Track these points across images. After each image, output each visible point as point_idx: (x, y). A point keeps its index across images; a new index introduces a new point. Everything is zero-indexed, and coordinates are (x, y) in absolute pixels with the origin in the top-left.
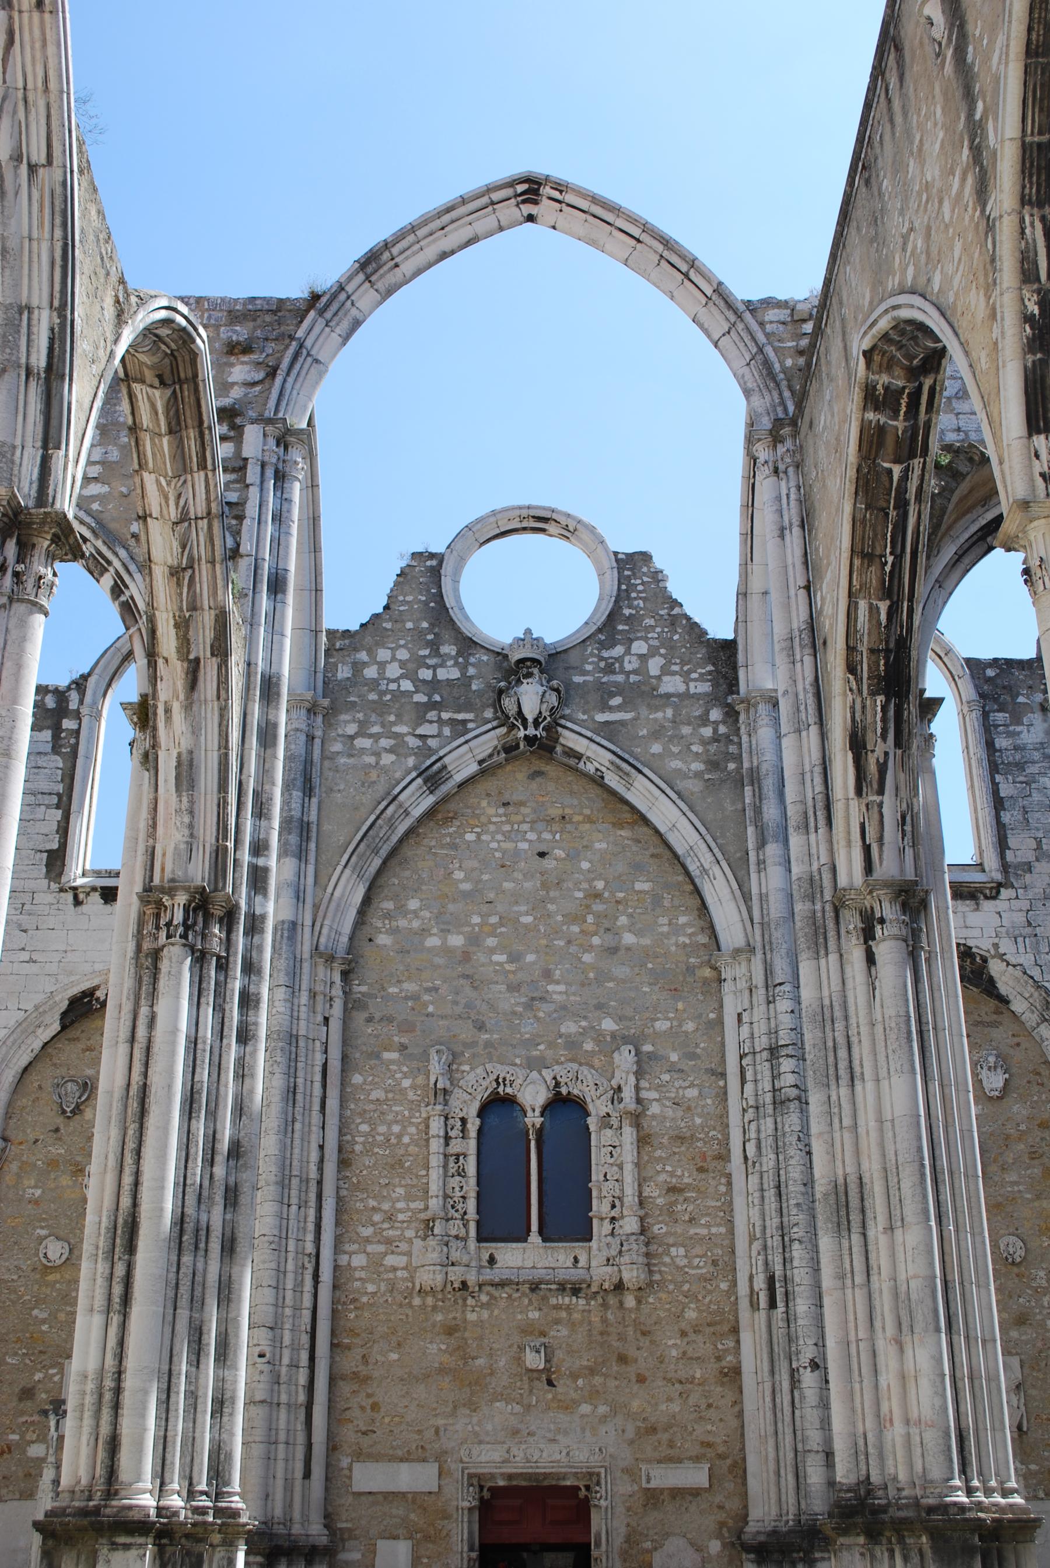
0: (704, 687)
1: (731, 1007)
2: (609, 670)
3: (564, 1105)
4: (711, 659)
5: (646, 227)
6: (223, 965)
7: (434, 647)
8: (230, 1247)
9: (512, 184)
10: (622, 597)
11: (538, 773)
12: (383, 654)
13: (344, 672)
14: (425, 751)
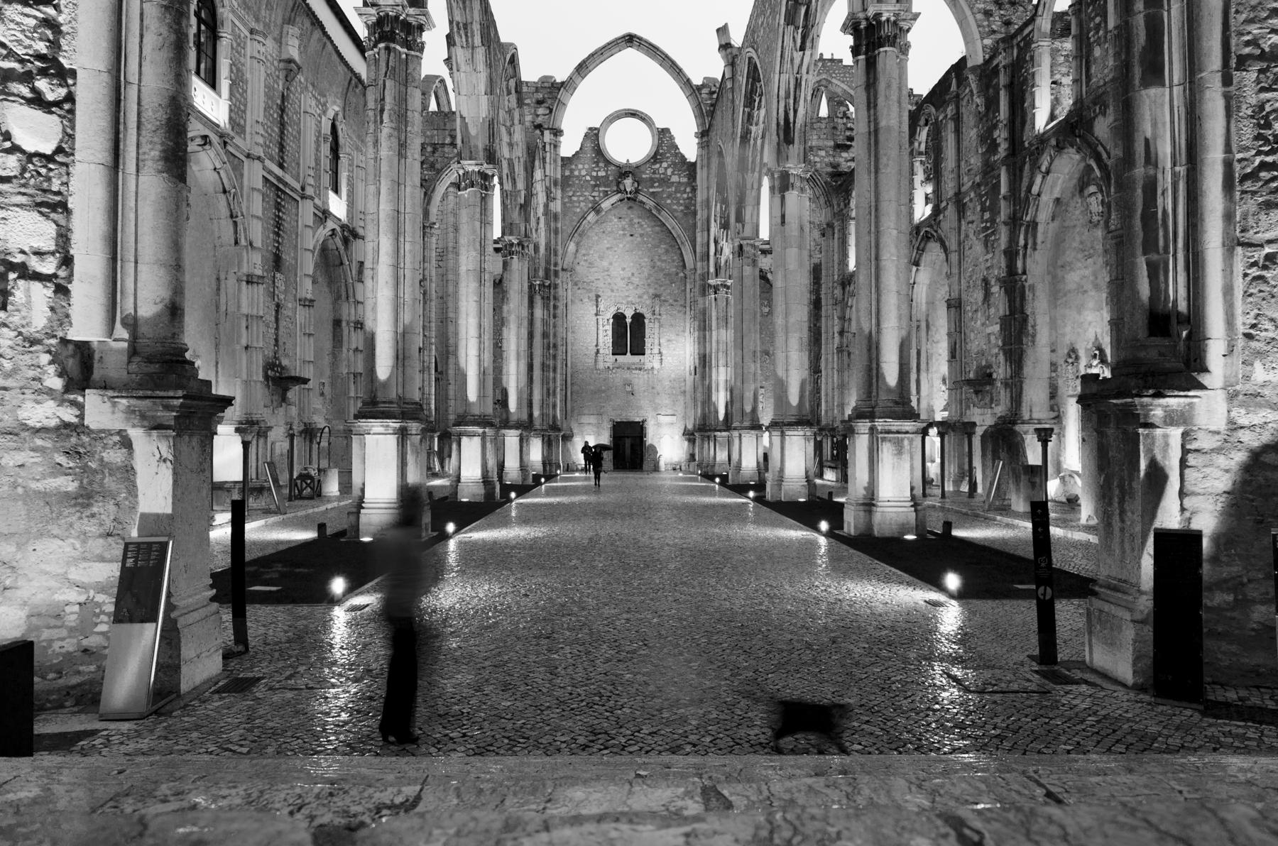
0: (685, 180)
1: (688, 287)
2: (654, 173)
3: (638, 318)
4: (688, 169)
5: (667, 56)
6: (548, 298)
7: (597, 163)
8: (555, 370)
9: (624, 37)
10: (659, 146)
11: (630, 208)
12: (580, 166)
13: (567, 173)
14: (595, 202)
